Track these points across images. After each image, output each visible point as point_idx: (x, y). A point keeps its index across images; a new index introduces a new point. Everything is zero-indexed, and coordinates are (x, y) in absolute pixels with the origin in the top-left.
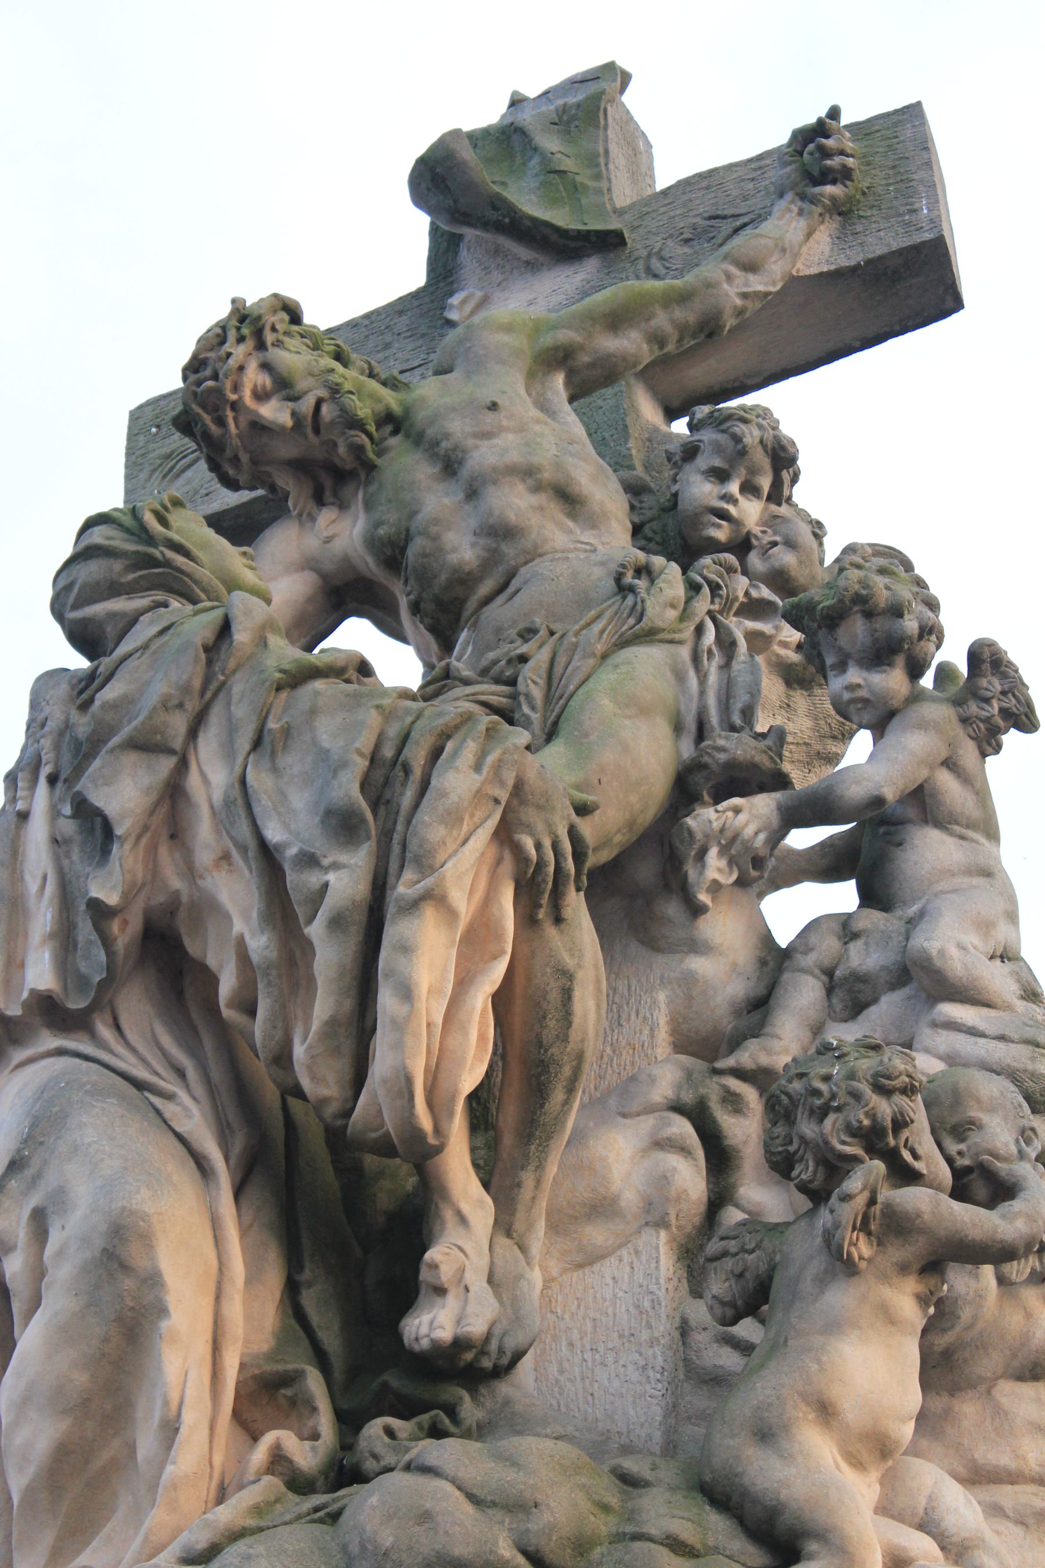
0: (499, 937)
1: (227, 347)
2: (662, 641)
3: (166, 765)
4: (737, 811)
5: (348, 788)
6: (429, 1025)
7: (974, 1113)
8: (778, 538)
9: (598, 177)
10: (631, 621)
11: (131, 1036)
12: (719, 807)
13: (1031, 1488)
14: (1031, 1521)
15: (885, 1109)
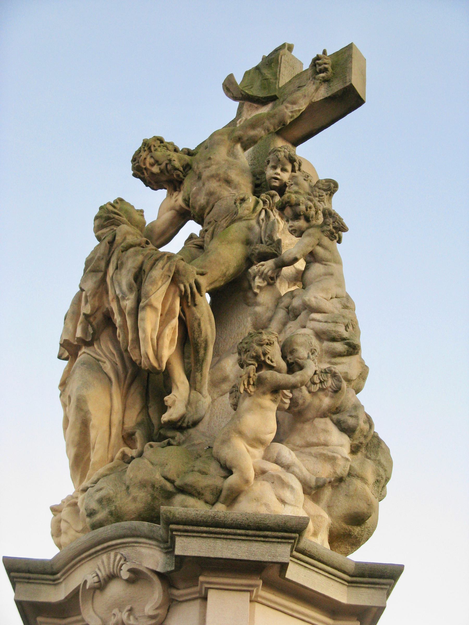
0: (174, 312)
1: (141, 154)
2: (244, 220)
3: (101, 274)
4: (263, 265)
5: (130, 277)
6: (152, 339)
7: (296, 347)
8: (293, 183)
9: (276, 79)
10: (235, 216)
11: (103, 347)
12: (257, 265)
13: (322, 447)
14: (318, 456)
15: (260, 350)
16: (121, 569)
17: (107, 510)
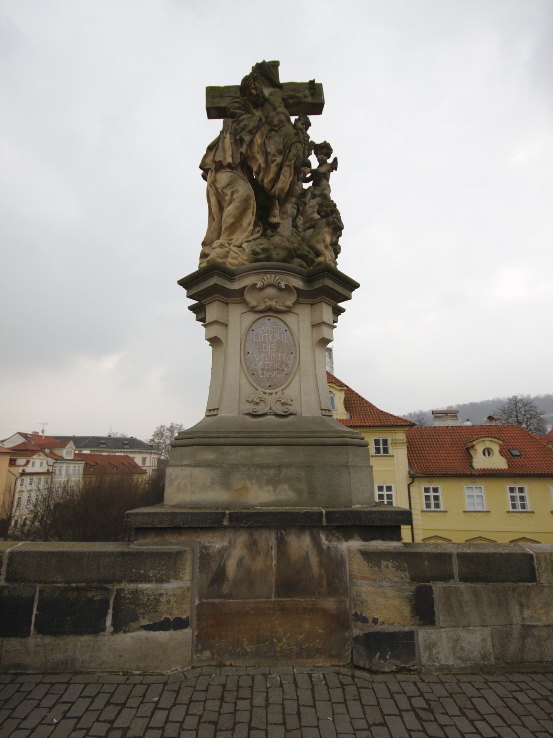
16: (279, 283)
17: (265, 255)
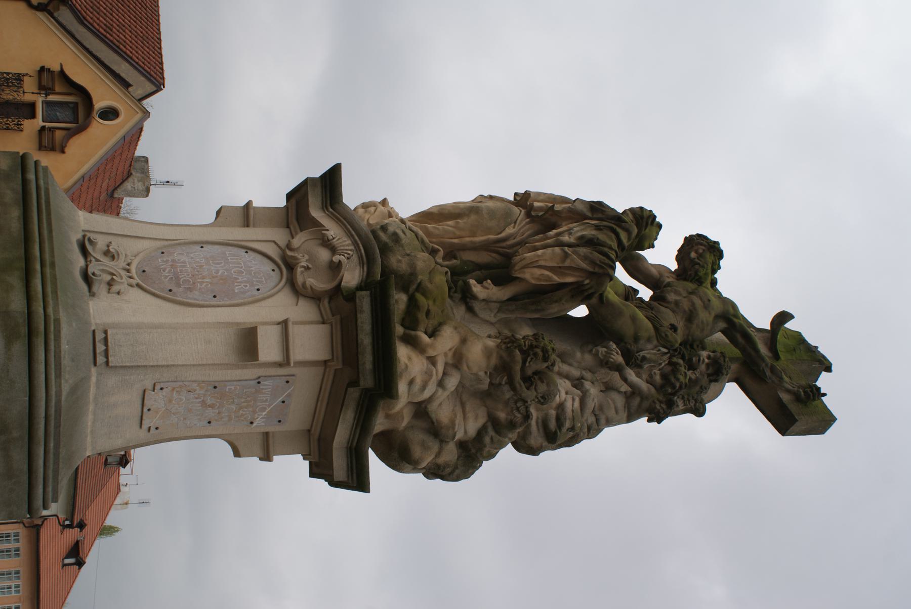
4: (617, 353)
